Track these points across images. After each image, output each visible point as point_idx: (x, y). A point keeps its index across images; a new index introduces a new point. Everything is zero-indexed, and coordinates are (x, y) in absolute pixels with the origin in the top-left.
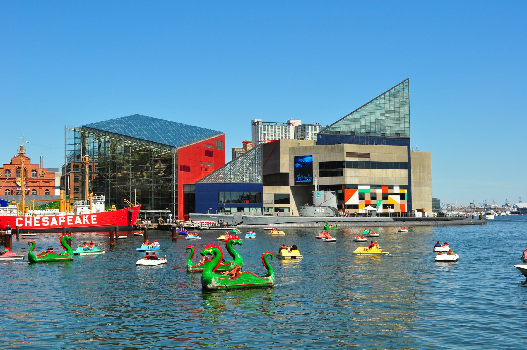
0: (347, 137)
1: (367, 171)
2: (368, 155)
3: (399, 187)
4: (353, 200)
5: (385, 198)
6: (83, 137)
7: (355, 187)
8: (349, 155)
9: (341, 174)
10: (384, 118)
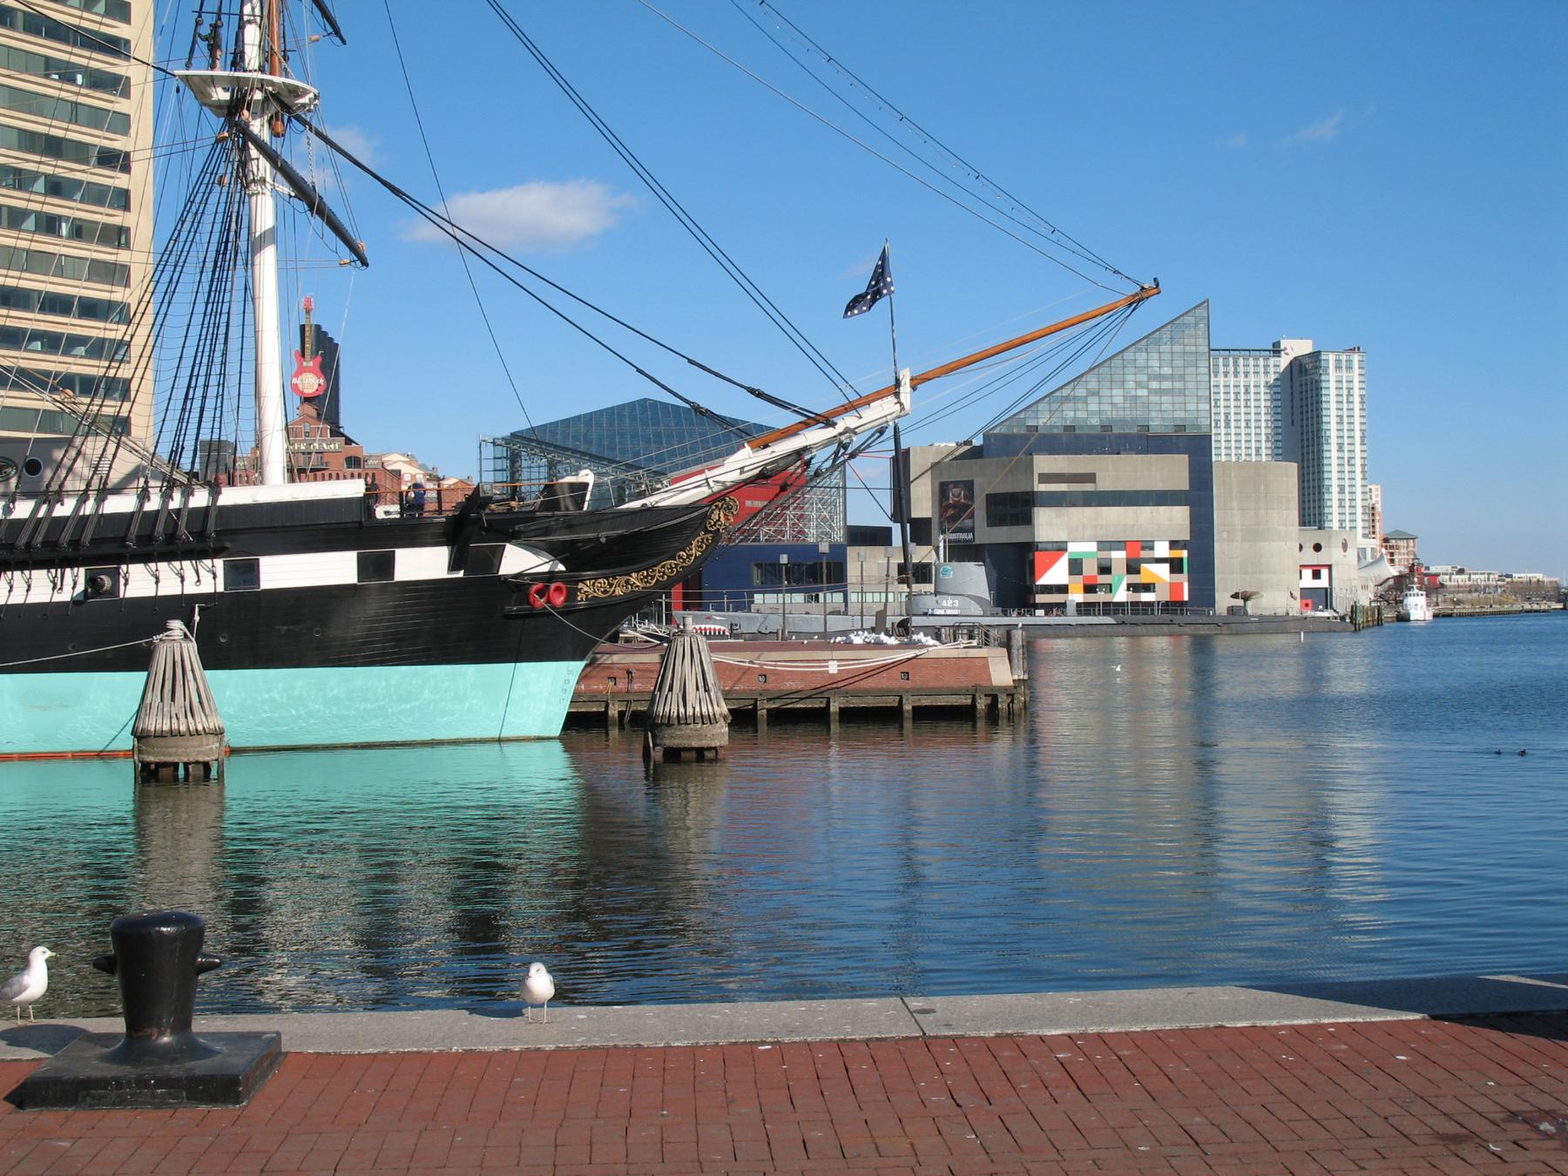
0: (1054, 437)
1: (1089, 511)
2: (1091, 478)
3: (1167, 544)
4: (1056, 574)
5: (1133, 568)
6: (514, 458)
7: (1061, 548)
8: (1046, 478)
9: (1028, 520)
10: (1145, 392)
